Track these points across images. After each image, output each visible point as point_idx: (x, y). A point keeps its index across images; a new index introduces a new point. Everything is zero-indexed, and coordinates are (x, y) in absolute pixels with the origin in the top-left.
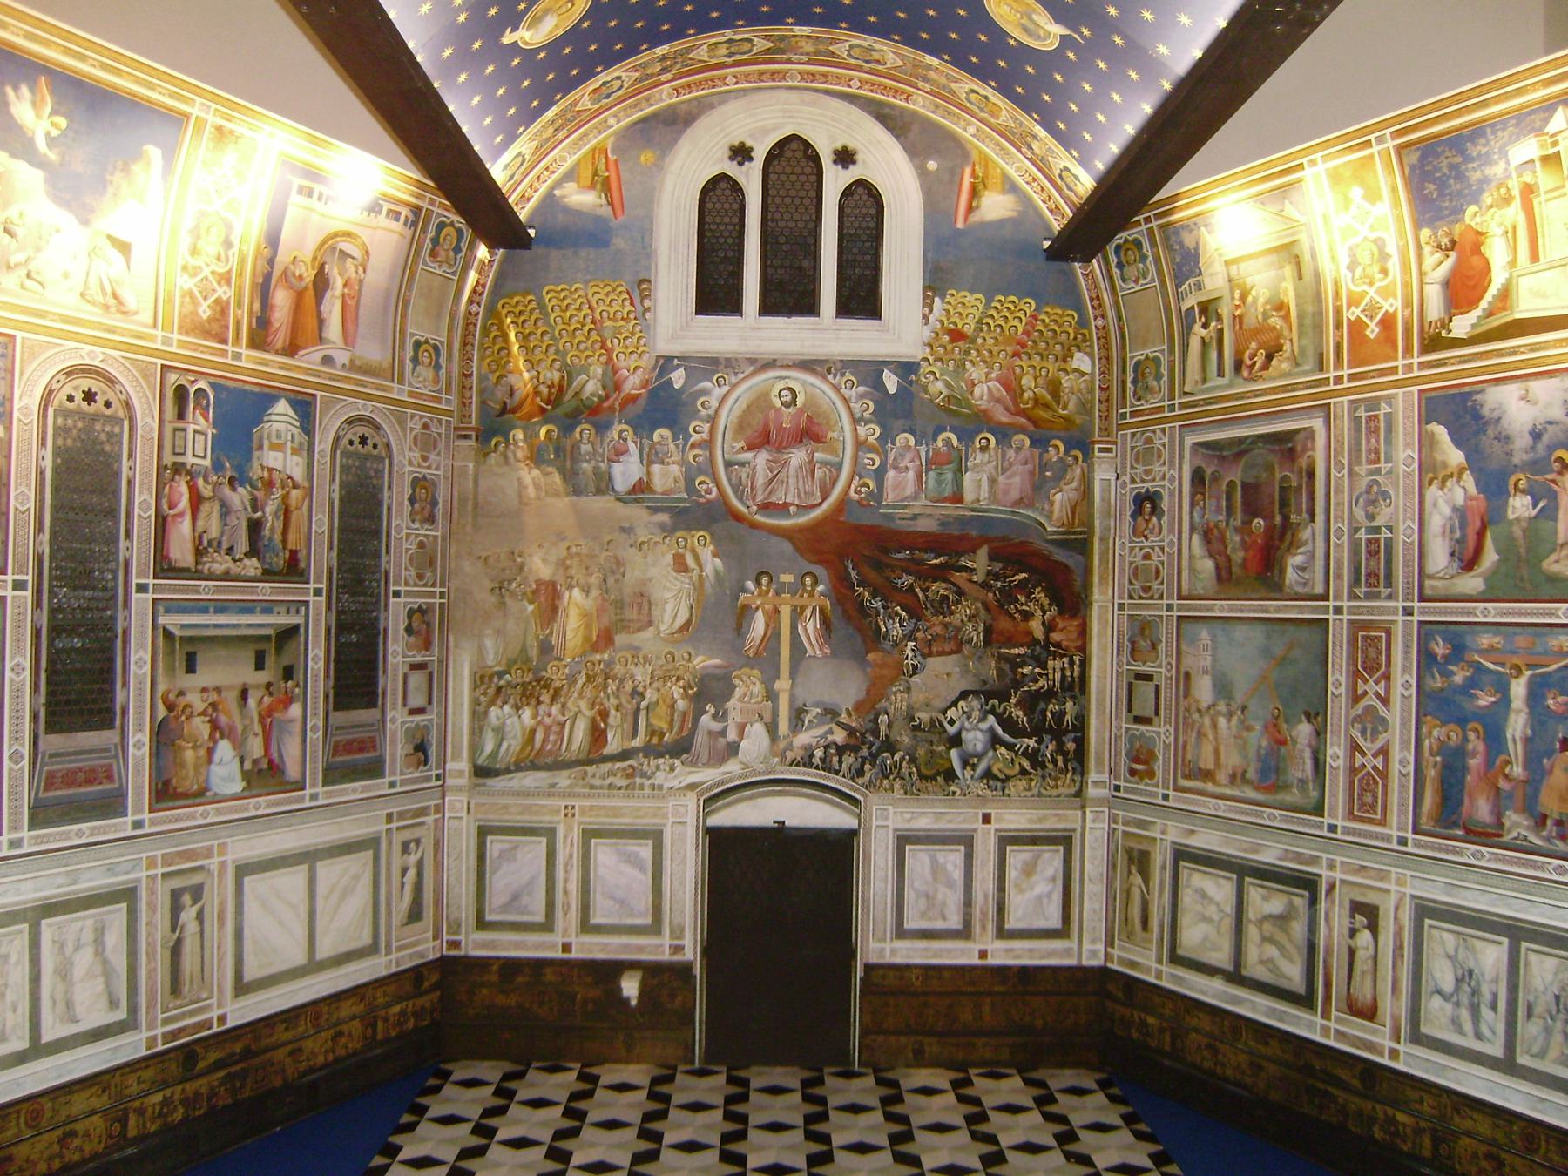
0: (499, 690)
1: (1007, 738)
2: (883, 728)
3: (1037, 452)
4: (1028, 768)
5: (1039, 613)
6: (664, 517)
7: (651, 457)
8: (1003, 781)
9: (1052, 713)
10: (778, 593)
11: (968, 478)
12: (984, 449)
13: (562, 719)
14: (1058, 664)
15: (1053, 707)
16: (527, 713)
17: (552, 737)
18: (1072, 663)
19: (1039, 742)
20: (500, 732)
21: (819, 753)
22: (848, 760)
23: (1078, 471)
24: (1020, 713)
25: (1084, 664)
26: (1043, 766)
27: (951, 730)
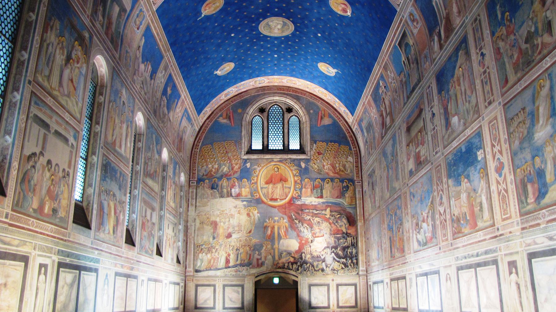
0: (202, 249)
1: (338, 259)
2: (303, 257)
3: (341, 184)
4: (344, 267)
5: (344, 225)
6: (245, 203)
7: (240, 187)
8: (337, 271)
9: (349, 252)
10: (274, 222)
11: (324, 191)
12: (327, 183)
13: (218, 256)
14: (350, 239)
15: (349, 250)
16: (209, 255)
17: (216, 261)
18: (354, 238)
19: (346, 260)
20: (202, 261)
21: (286, 265)
22: (295, 266)
23: (352, 188)
24: (341, 252)
25: (356, 238)
26: (348, 267)
27: (322, 257)
